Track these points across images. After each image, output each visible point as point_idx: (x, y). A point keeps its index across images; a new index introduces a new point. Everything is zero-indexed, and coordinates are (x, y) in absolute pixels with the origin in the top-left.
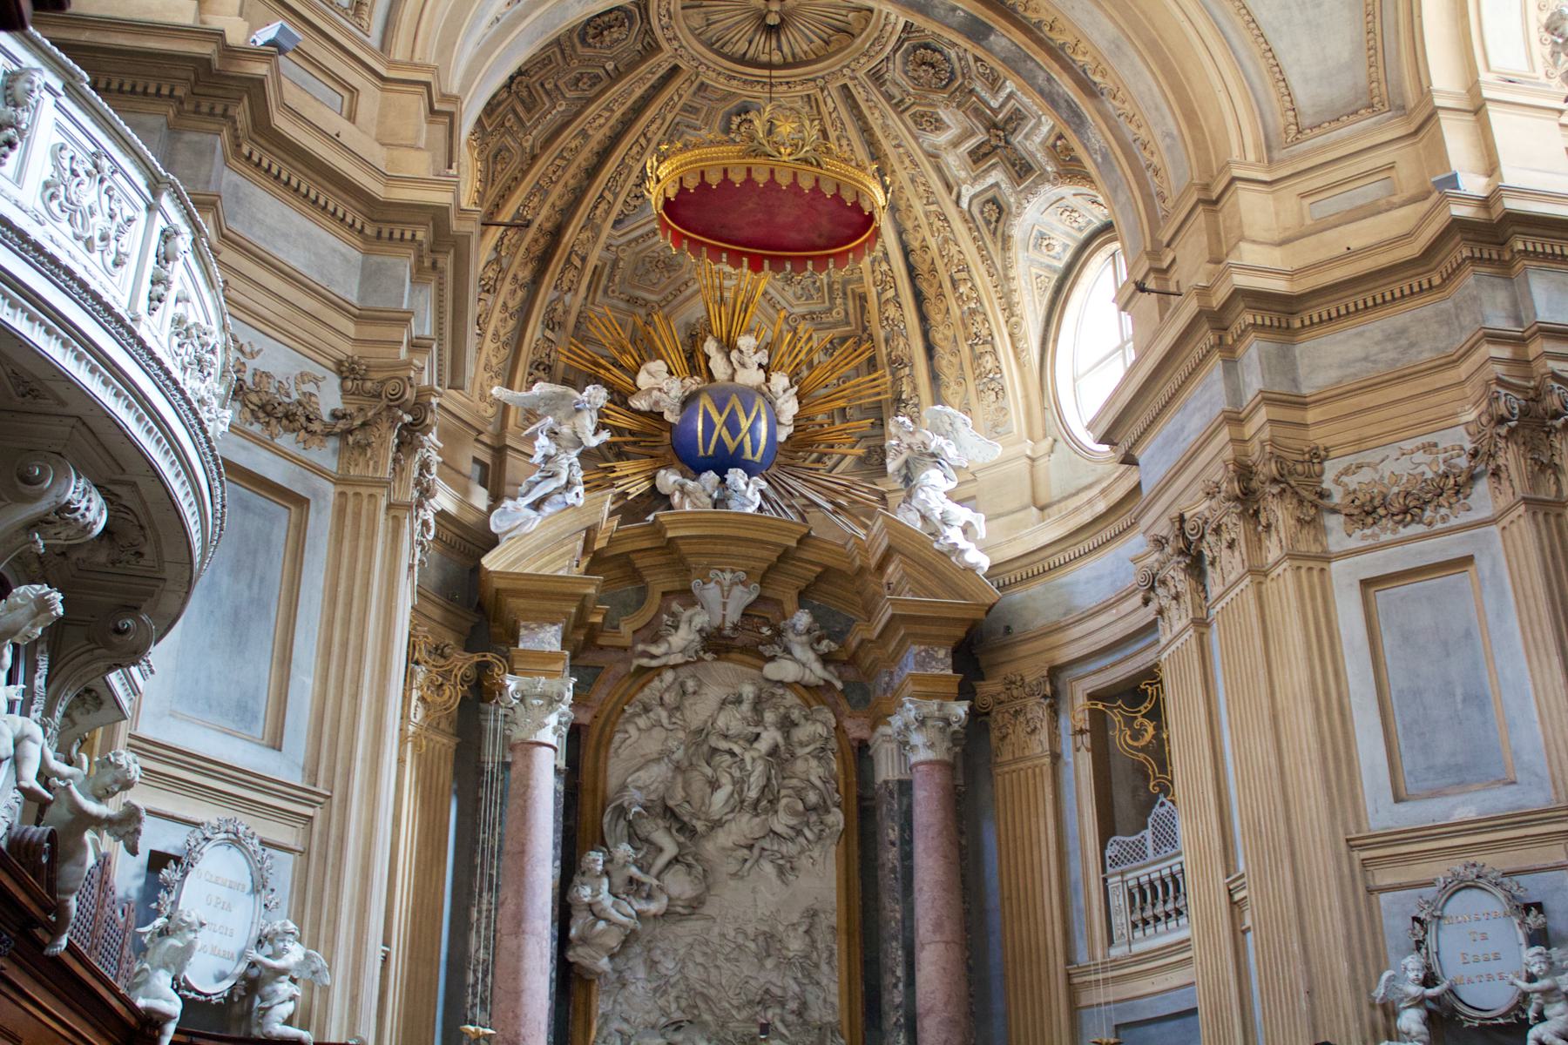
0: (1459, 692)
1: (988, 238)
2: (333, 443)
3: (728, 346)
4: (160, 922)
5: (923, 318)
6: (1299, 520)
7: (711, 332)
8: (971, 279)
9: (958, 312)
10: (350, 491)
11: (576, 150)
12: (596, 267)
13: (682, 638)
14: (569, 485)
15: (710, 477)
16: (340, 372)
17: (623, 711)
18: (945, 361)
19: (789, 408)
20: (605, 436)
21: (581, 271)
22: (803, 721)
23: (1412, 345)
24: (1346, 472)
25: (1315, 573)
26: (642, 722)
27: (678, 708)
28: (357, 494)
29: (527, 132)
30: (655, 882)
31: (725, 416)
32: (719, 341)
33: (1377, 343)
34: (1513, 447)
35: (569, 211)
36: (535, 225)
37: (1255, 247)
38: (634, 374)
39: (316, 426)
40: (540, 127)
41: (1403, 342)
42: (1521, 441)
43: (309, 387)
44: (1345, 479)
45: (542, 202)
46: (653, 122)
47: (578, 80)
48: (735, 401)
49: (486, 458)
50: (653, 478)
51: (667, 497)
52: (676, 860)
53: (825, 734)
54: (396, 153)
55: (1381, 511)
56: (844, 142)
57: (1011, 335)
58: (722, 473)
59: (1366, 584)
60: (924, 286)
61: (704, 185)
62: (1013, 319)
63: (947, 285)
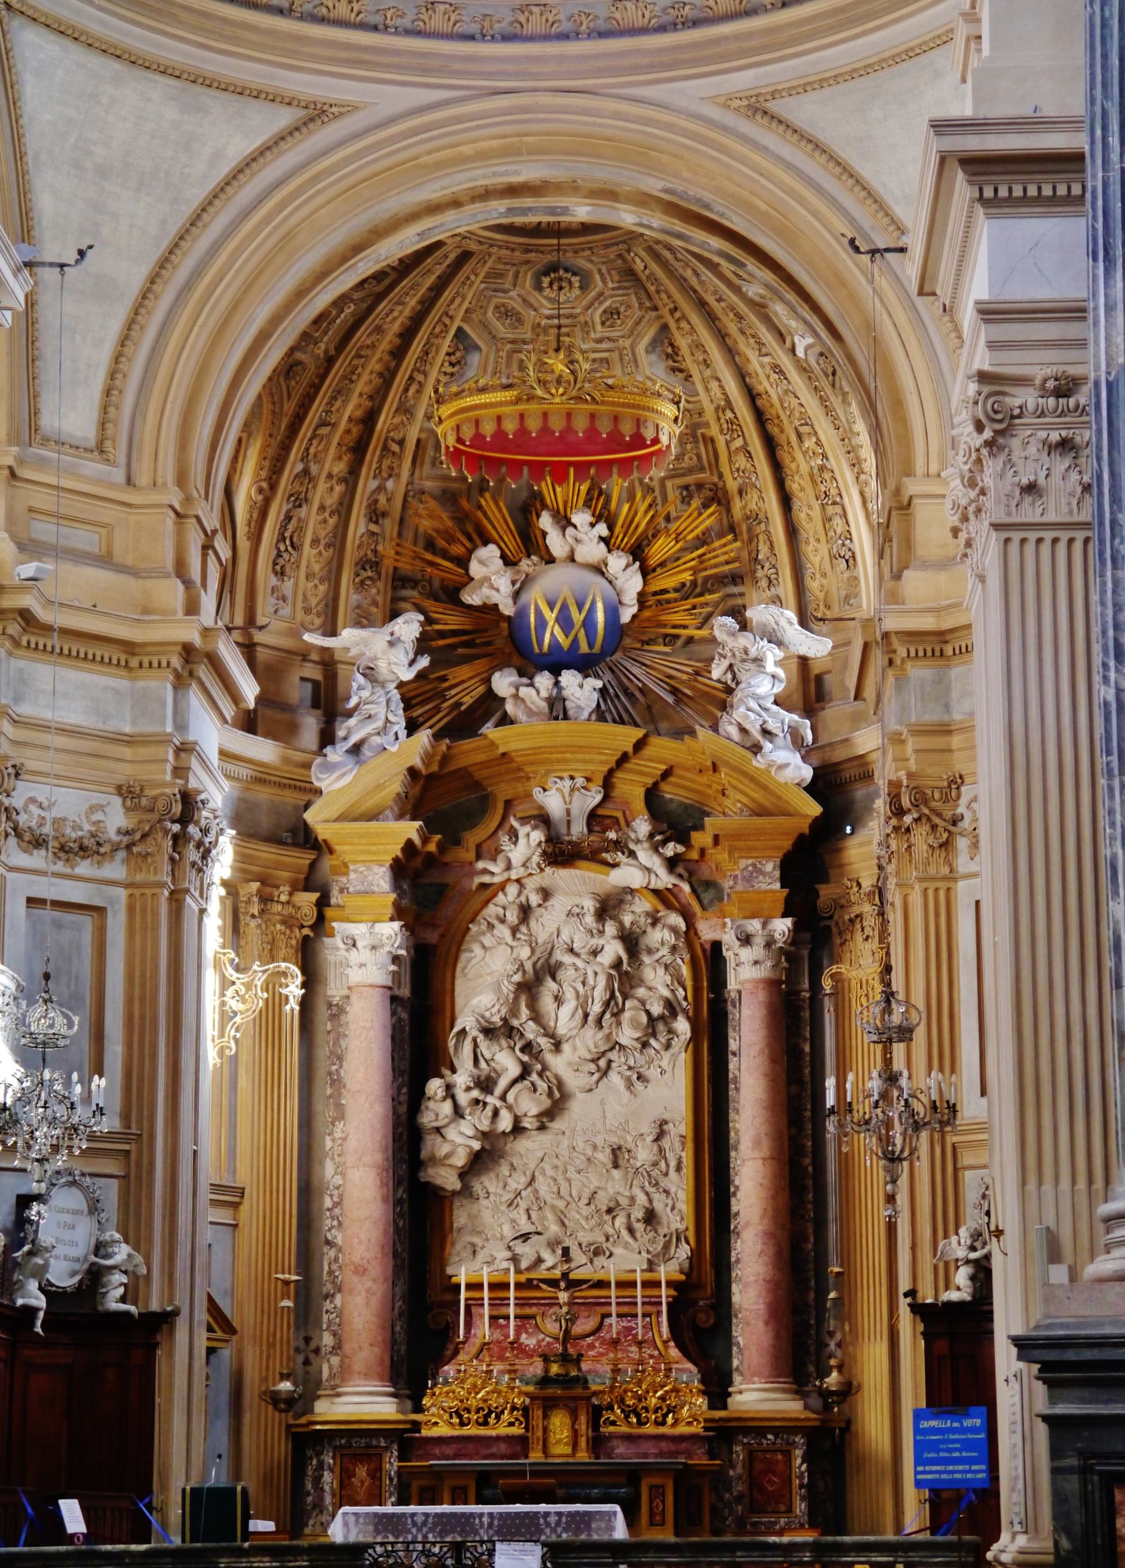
1: (829, 390)
2: (121, 854)
3: (564, 522)
4: (26, 1248)
7: (544, 506)
8: (816, 434)
10: (137, 892)
11: (373, 346)
12: (419, 441)
15: (544, 680)
16: (120, 794)
20: (424, 662)
21: (400, 457)
26: (487, 940)
30: (498, 1104)
31: (556, 611)
35: (379, 396)
38: (463, 562)
43: (98, 816)
44: (974, 805)
45: (345, 402)
46: (452, 301)
50: (488, 681)
51: (503, 700)
52: (521, 1077)
54: (149, 583)
56: (664, 296)
57: (862, 494)
58: (556, 672)
60: (774, 430)
61: (478, 437)
62: (863, 477)
63: (793, 438)
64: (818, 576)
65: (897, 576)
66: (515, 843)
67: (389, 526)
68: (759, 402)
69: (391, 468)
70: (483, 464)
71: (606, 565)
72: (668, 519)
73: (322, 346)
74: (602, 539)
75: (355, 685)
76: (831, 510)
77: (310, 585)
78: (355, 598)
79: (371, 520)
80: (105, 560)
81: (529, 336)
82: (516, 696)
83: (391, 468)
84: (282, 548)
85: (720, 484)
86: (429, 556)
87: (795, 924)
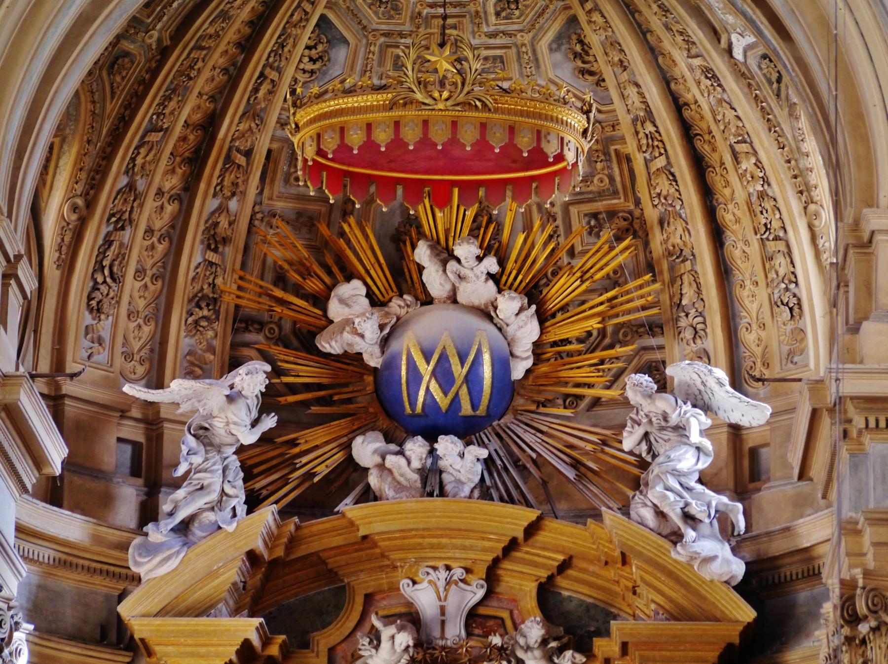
1: (772, 101)
5: (707, 192)
7: (421, 235)
8: (755, 153)
11: (217, 36)
12: (270, 151)
15: (416, 447)
18: (735, 251)
20: (270, 422)
21: (247, 172)
38: (321, 301)
40: (165, 18)
45: (181, 104)
49: (140, 438)
50: (347, 447)
57: (811, 227)
58: (431, 437)
60: (704, 148)
61: (343, 149)
62: (812, 207)
63: (728, 158)
64: (754, 327)
65: (854, 329)
66: (377, 647)
67: (231, 254)
68: (686, 114)
69: (235, 185)
70: (348, 181)
71: (496, 308)
72: (571, 253)
73: (155, 34)
74: (490, 276)
75: (184, 449)
76: (772, 246)
77: (132, 325)
78: (187, 342)
79: (209, 247)
81: (407, 27)
82: (382, 467)
83: (235, 185)
84: (100, 279)
85: (637, 213)
86: (279, 293)
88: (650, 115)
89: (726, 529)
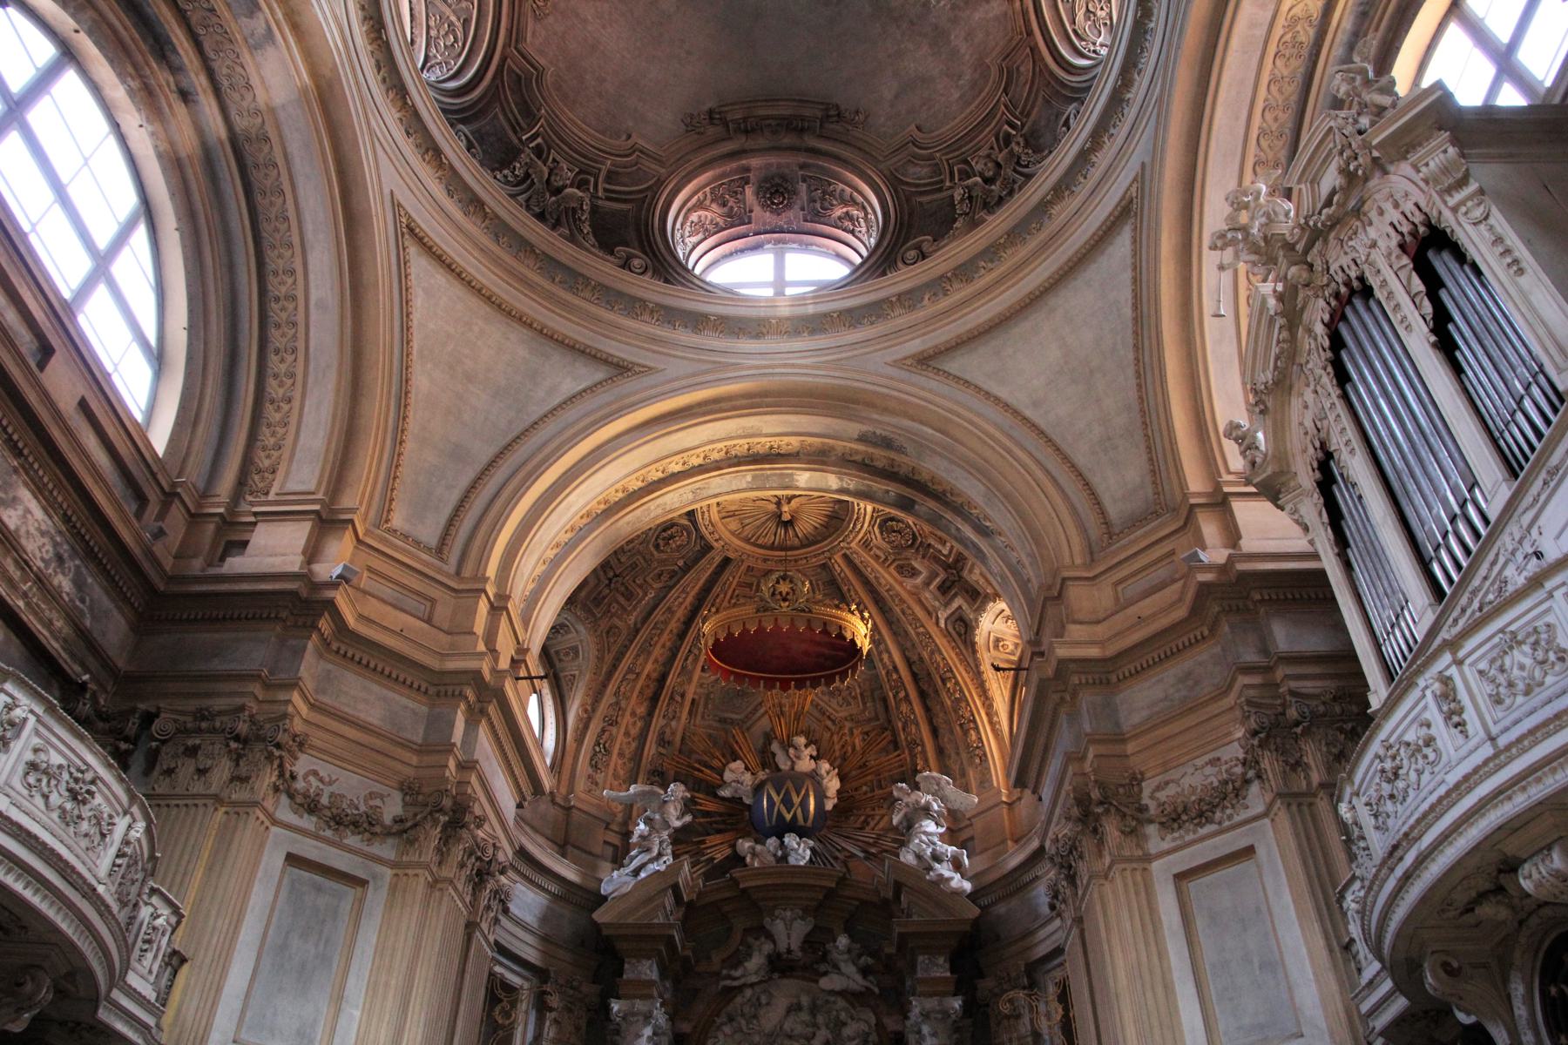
0: (1256, 960)
2: (390, 841)
3: (787, 744)
5: (927, 709)
6: (1123, 832)
8: (955, 677)
9: (949, 703)
10: (400, 872)
11: (666, 623)
12: (693, 700)
13: (755, 962)
14: (660, 855)
15: (772, 842)
17: (714, 1021)
18: (945, 739)
19: (833, 785)
20: (688, 818)
21: (682, 705)
22: (849, 1021)
23: (1197, 683)
24: (1158, 788)
25: (1138, 873)
27: (755, 1017)
28: (406, 875)
29: (630, 613)
32: (782, 743)
33: (1172, 686)
34: (1267, 753)
36: (644, 676)
37: (1078, 627)
39: (378, 829)
41: (1190, 683)
42: (1273, 747)
43: (378, 802)
44: (1158, 795)
47: (660, 575)
48: (789, 784)
50: (733, 846)
53: (867, 1030)
54: (456, 638)
55: (1184, 817)
59: (1181, 877)
61: (730, 635)
73: (633, 618)
80: (429, 621)
82: (754, 854)
87: (964, 1001)
88: (895, 668)
89: (957, 865)
